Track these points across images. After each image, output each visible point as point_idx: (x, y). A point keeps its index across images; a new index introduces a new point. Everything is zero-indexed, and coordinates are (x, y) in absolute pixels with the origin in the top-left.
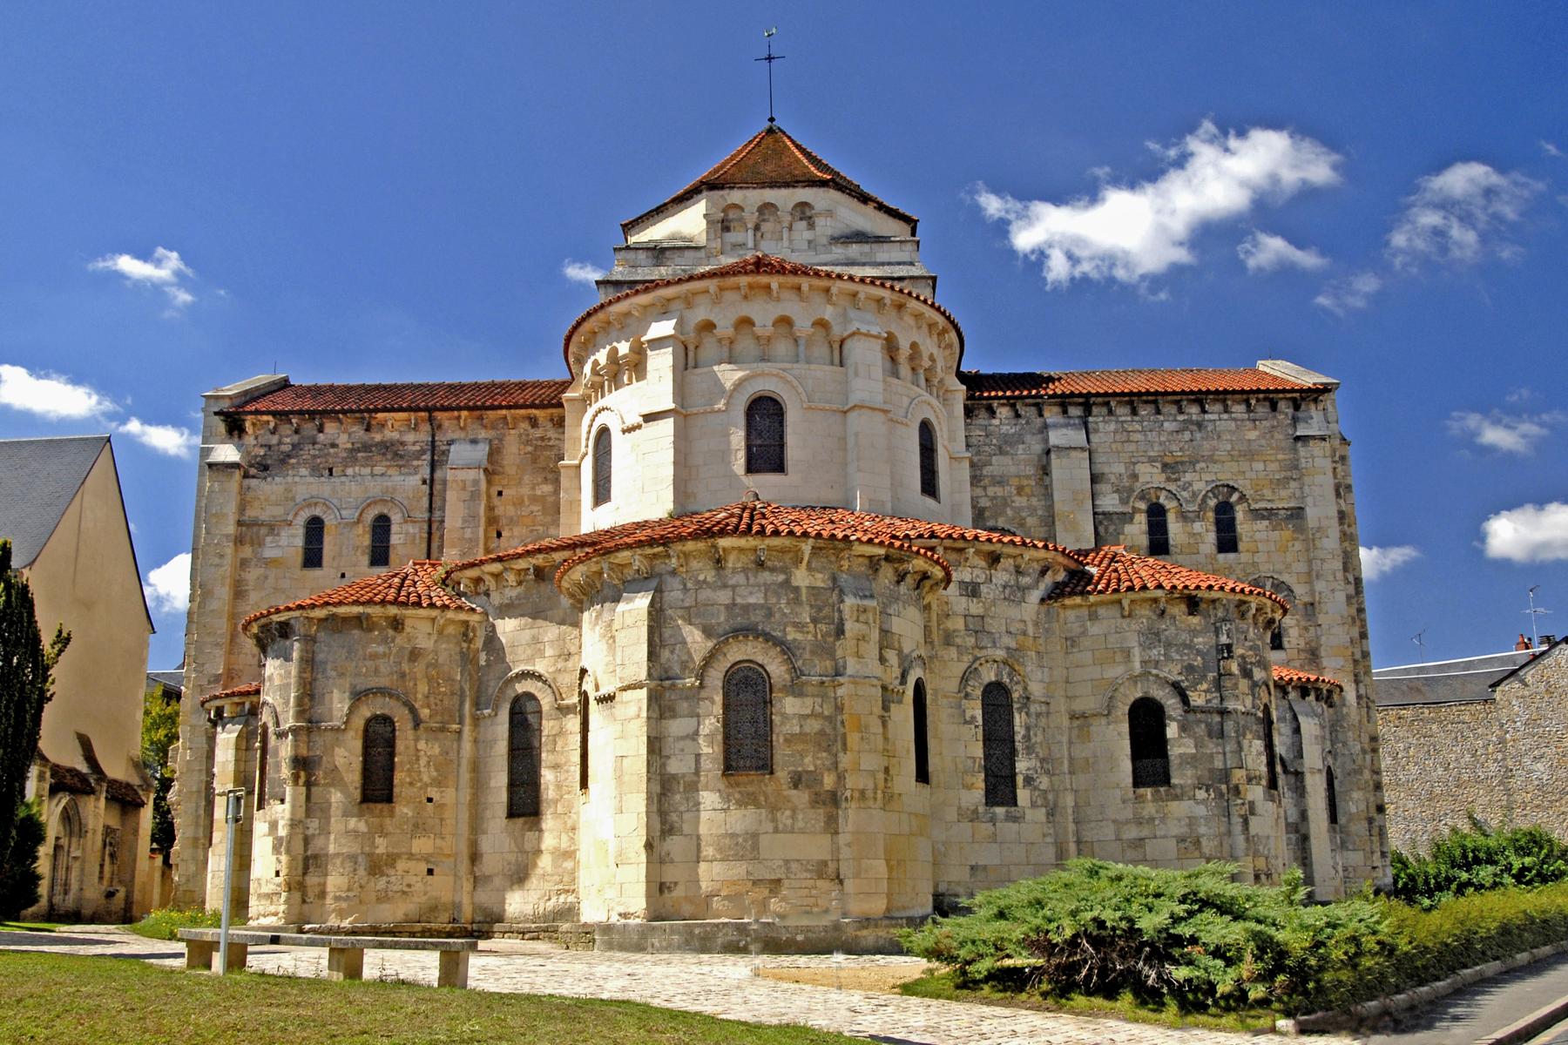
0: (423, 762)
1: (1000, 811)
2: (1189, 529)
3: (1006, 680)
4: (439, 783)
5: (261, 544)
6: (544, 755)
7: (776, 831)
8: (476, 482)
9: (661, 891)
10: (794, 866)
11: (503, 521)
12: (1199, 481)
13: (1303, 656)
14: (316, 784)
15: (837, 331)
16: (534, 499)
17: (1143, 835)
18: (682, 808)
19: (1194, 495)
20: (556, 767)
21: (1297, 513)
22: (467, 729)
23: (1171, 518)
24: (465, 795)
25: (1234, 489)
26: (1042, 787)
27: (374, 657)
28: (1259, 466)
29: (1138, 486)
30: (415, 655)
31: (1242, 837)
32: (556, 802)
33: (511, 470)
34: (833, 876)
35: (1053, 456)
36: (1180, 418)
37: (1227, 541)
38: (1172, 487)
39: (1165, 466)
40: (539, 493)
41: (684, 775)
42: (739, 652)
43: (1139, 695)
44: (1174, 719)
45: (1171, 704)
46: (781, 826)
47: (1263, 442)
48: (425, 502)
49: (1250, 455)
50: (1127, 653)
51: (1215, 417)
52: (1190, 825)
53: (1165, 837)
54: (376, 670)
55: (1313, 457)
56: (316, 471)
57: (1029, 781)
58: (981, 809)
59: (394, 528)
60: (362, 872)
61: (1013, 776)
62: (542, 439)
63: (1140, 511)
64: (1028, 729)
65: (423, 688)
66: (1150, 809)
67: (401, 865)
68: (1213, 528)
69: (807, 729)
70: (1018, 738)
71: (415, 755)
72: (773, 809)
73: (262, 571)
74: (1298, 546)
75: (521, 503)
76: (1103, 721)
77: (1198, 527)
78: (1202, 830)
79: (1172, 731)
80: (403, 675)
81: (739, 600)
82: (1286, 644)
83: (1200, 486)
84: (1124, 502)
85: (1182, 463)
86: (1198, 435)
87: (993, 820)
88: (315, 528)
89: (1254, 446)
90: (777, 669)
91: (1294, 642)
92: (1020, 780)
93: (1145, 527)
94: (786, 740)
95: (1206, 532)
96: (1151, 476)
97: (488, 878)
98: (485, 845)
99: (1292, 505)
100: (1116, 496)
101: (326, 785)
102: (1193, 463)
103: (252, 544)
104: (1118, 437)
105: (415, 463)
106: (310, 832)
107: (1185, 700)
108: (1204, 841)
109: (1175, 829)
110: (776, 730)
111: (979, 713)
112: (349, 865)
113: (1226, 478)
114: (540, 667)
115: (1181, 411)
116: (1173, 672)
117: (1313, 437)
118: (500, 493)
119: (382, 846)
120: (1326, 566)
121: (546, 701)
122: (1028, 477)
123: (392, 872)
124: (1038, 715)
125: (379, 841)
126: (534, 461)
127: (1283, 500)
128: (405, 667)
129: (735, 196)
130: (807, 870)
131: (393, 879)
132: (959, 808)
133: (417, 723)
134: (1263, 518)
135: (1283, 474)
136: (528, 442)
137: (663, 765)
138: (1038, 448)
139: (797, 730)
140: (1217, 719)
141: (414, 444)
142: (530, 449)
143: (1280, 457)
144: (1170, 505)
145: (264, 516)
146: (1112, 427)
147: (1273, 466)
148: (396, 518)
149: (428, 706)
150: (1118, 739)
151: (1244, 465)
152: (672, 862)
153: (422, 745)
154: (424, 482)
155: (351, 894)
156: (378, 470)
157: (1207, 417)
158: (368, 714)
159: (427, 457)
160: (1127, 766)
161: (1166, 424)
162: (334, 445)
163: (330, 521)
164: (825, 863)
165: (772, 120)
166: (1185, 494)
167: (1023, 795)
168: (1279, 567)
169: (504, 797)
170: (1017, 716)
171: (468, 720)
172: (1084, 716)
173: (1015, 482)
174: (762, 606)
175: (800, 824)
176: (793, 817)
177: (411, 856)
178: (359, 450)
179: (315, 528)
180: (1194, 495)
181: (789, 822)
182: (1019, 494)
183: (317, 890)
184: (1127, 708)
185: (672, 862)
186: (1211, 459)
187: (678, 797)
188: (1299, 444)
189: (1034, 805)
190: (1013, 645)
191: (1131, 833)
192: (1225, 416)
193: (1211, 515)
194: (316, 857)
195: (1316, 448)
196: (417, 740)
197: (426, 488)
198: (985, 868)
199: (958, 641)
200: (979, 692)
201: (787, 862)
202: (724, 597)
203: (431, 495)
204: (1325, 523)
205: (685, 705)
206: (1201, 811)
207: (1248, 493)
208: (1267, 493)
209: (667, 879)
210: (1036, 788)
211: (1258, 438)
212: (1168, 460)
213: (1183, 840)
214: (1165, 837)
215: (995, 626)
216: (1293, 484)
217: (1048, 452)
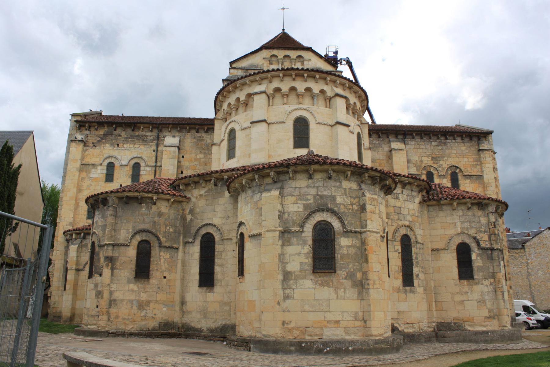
0: (162, 260)
1: (408, 288)
4: (169, 271)
5: (90, 172)
6: (216, 260)
7: (337, 298)
8: (175, 152)
9: (283, 325)
10: (345, 314)
11: (184, 167)
12: (445, 164)
14: (116, 268)
15: (330, 94)
16: (196, 160)
17: (463, 299)
18: (294, 287)
19: (443, 169)
20: (221, 265)
21: (480, 177)
22: (181, 248)
24: (178, 276)
25: (457, 167)
27: (142, 215)
28: (466, 160)
29: (423, 165)
30: (160, 215)
31: (502, 301)
32: (221, 280)
33: (187, 148)
34: (361, 319)
35: (393, 152)
36: (438, 141)
38: (435, 166)
39: (433, 158)
40: (198, 157)
41: (294, 272)
42: (319, 217)
43: (460, 241)
44: (474, 252)
45: (473, 245)
46: (339, 296)
48: (154, 159)
50: (455, 224)
51: (450, 141)
52: (482, 295)
53: (472, 300)
54: (144, 221)
55: (485, 157)
56: (112, 145)
57: (417, 276)
58: (401, 288)
59: (142, 168)
60: (135, 307)
61: (412, 274)
62: (200, 137)
63: (424, 174)
65: (163, 229)
66: (466, 289)
67: (152, 305)
68: (450, 181)
69: (350, 252)
70: (414, 258)
71: (160, 260)
72: (336, 289)
73: (89, 182)
75: (191, 161)
76: (446, 252)
78: (486, 297)
79: (474, 256)
80: (155, 222)
81: (319, 193)
83: (445, 166)
84: (417, 170)
85: (439, 157)
86: (444, 147)
87: (405, 292)
88: (111, 167)
89: (464, 152)
90: (336, 224)
94: (341, 257)
96: (427, 161)
97: (190, 312)
98: (188, 298)
99: (478, 174)
100: (415, 168)
101: (120, 269)
102: (443, 157)
103: (86, 172)
104: (416, 147)
105: (151, 144)
106: (113, 289)
107: (478, 244)
108: (487, 302)
109: (476, 296)
110: (337, 252)
112: (129, 305)
113: (454, 163)
114: (216, 221)
115: (438, 139)
116: (472, 232)
117: (485, 150)
118: (183, 157)
119: (144, 297)
121: (217, 237)
122: (383, 160)
123: (148, 308)
124: (420, 249)
125: (142, 294)
126: (197, 145)
127: (475, 172)
128: (156, 219)
129: (275, 52)
130: (351, 316)
131: (148, 311)
132: (393, 287)
133: (160, 243)
134: (468, 178)
135: (475, 163)
136: (195, 138)
137: (284, 267)
138: (386, 148)
139: (346, 252)
140: (490, 252)
141: (151, 137)
142: (195, 140)
143: (474, 156)
144: (435, 172)
145: (92, 161)
146: (413, 143)
147: (471, 160)
148: (142, 164)
149: (165, 237)
150: (450, 261)
151: (461, 159)
152: (289, 311)
153: (162, 253)
154: (154, 151)
155: (130, 317)
156: (136, 146)
157: (447, 141)
158: (139, 239)
159: (155, 142)
160: (455, 271)
161: (433, 143)
162: (120, 136)
163: (117, 164)
164: (357, 313)
165: (283, 30)
167: (416, 282)
169: (197, 277)
171: (181, 244)
172: (437, 250)
173: (378, 161)
174: (330, 196)
175: (348, 295)
176: (344, 292)
177: (156, 302)
178: (129, 138)
179: (111, 167)
180: (443, 169)
181: (343, 294)
183: (115, 315)
184: (455, 247)
185: (289, 311)
186: (449, 156)
187: (292, 282)
188: (481, 152)
189: (419, 286)
190: (411, 220)
191: (458, 298)
192: (454, 141)
193: (449, 176)
194: (115, 300)
195: (487, 154)
196: (160, 251)
197: (154, 153)
199: (392, 217)
200: (399, 239)
201: (342, 312)
202: (313, 191)
203: (156, 157)
204: (490, 181)
205: (295, 239)
206: (485, 289)
207: (463, 169)
208: (469, 169)
209: (287, 320)
213: (479, 302)
214: (472, 300)
216: (478, 167)
217: (391, 151)
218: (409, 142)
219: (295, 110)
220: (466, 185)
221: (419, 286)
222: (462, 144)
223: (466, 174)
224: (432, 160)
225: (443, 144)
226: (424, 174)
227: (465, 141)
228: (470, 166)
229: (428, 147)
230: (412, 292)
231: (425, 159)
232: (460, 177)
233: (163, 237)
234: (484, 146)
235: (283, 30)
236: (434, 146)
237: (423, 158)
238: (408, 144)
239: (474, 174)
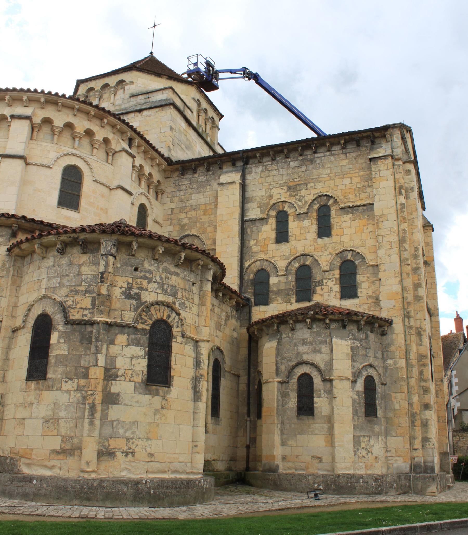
2: (301, 225)
12: (308, 195)
13: (370, 301)
23: (291, 218)
25: (329, 197)
28: (347, 181)
36: (300, 158)
37: (324, 229)
38: (292, 200)
39: (289, 188)
47: (351, 166)
49: (342, 175)
51: (322, 155)
55: (380, 171)
63: (272, 217)
68: (315, 222)
74: (370, 228)
77: (306, 223)
82: (359, 294)
83: (310, 198)
84: (262, 212)
85: (299, 185)
86: (310, 167)
89: (345, 169)
91: (364, 292)
93: (274, 226)
95: (311, 225)
96: (280, 194)
100: (259, 209)
102: (306, 184)
117: (380, 158)
120: (385, 239)
127: (362, 200)
134: (348, 213)
144: (290, 211)
146: (260, 169)
147: (358, 180)
151: (338, 182)
157: (316, 155)
166: (300, 204)
168: (357, 243)
173: (203, 207)
180: (305, 202)
182: (204, 214)
186: (318, 180)
192: (328, 154)
193: (315, 215)
204: (385, 211)
207: (340, 197)
208: (352, 197)
211: (349, 164)
212: (291, 184)
218: (253, 169)
219: (73, 155)
220: (344, 225)
222: (343, 156)
223: (343, 206)
224: (288, 191)
225: (308, 163)
226: (272, 217)
227: (348, 151)
228: (355, 190)
229: (283, 171)
231: (275, 191)
232: (333, 213)
234: (379, 152)
235: (151, 53)
236: (294, 168)
237: (273, 191)
238: (251, 173)
239: (358, 203)
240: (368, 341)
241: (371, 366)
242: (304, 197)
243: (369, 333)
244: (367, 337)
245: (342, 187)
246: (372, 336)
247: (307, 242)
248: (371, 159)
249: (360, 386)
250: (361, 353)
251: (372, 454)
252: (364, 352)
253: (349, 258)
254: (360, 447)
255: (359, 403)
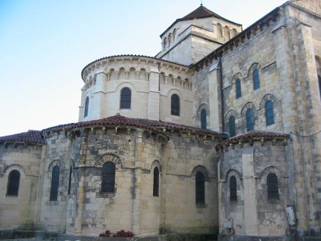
1: (53, 202)
2: (246, 85)
3: (59, 165)
23: (241, 82)
26: (65, 195)
57: (61, 193)
64: (63, 178)
87: (51, 205)
92: (59, 193)
111: (51, 175)
167: (59, 198)
170: (60, 175)
189: (62, 200)
190: (62, 155)
198: (48, 218)
208: (268, 60)
210: (63, 195)
215: (58, 150)
220: (265, 78)
221: (62, 200)
230: (55, 204)
232: (260, 73)
233: (281, 191)
240: (270, 152)
241: (272, 167)
242: (246, 68)
243: (271, 146)
244: (269, 149)
245: (262, 55)
246: (273, 148)
247: (249, 95)
248: (273, 32)
249: (264, 181)
250: (264, 160)
251: (275, 223)
252: (267, 159)
253: (269, 99)
254: (265, 218)
255: (263, 192)
